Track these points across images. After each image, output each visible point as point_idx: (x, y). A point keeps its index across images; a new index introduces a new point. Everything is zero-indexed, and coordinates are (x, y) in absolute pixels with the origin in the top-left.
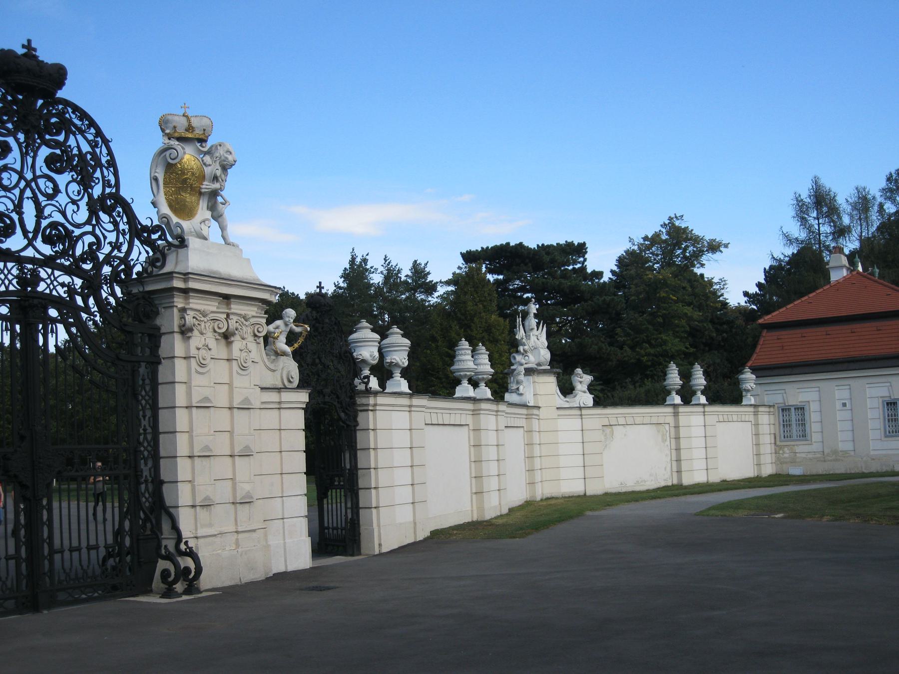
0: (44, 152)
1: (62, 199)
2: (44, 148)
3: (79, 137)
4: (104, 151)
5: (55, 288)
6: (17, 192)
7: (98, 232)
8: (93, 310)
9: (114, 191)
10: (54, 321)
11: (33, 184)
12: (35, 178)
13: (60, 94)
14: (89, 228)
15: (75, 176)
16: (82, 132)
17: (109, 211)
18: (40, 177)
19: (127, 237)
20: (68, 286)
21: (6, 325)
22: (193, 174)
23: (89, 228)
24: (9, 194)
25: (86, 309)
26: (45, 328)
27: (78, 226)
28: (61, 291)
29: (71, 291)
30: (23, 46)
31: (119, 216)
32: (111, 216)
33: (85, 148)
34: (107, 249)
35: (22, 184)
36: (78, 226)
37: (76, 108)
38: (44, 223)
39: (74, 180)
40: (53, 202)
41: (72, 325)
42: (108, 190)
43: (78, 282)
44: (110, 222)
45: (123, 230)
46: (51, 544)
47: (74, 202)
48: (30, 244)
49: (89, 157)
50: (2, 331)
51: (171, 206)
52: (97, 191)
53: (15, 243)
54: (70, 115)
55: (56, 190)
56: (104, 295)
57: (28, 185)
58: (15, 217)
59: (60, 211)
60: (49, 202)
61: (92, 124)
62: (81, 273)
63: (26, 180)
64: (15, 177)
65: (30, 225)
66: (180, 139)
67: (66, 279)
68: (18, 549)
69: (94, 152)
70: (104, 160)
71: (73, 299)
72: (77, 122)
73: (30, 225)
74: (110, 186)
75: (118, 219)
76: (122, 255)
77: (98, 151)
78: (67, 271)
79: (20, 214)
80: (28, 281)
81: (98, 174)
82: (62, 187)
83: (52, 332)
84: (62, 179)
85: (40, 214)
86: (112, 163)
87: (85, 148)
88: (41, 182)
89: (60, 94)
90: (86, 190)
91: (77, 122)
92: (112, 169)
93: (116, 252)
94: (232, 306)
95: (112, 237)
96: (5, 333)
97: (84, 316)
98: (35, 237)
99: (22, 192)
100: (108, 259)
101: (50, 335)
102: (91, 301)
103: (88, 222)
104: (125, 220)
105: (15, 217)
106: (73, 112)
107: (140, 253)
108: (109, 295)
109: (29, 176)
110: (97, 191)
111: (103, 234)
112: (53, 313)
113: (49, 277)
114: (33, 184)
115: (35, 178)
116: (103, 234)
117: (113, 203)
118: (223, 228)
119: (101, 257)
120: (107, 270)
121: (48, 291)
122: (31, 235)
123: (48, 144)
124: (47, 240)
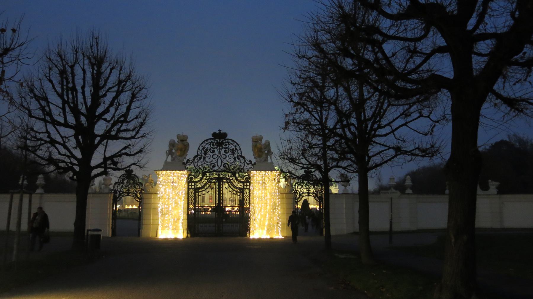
0: (223, 150)
1: (227, 158)
17: (239, 159)
33: (233, 147)
37: (231, 140)
52: (236, 156)
53: (216, 168)
54: (230, 141)
55: (226, 157)
58: (216, 164)
61: (235, 142)
62: (231, 172)
65: (219, 165)
72: (232, 142)
73: (219, 165)
84: (227, 155)
85: (222, 162)
86: (240, 149)
88: (223, 156)
91: (232, 142)
95: (240, 164)
100: (238, 169)
102: (234, 178)
105: (216, 164)
109: (219, 155)
110: (236, 156)
112: (225, 181)
118: (271, 158)
119: (236, 169)
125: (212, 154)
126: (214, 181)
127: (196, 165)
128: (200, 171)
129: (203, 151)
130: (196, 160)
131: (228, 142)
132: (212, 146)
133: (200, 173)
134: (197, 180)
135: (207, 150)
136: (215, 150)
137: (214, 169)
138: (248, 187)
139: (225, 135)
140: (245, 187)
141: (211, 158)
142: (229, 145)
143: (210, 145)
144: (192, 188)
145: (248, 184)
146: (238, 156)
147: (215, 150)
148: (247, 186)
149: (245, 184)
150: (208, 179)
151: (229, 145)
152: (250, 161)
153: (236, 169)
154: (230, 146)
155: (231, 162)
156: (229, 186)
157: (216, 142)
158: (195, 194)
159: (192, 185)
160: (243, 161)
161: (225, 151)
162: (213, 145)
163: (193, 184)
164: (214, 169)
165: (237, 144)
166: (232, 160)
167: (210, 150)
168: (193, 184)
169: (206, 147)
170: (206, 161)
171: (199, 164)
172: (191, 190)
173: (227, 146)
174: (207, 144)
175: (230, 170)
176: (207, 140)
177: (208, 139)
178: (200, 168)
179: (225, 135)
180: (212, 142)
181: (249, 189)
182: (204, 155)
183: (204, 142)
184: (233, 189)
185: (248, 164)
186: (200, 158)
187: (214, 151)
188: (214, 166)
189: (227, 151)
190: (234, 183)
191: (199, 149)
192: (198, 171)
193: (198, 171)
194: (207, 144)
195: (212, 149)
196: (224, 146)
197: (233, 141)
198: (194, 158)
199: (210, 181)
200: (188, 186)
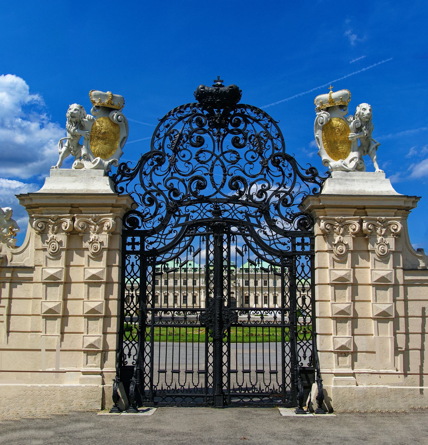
0: (230, 137)
1: (242, 162)
2: (229, 134)
3: (255, 124)
4: (274, 128)
5: (235, 214)
6: (210, 163)
7: (267, 178)
8: (262, 226)
9: (281, 151)
10: (234, 234)
11: (221, 158)
12: (223, 153)
13: (240, 102)
14: (262, 176)
15: (252, 148)
16: (257, 121)
17: (276, 164)
18: (226, 152)
19: (292, 178)
20: (246, 212)
21: (203, 238)
22: (339, 130)
23: (262, 176)
24: (204, 165)
25: (259, 226)
26: (229, 238)
27: (254, 177)
28: (240, 217)
29: (248, 215)
30: (215, 81)
31: (284, 166)
32: (277, 166)
33: (259, 129)
34: (274, 188)
35: (214, 158)
36: (254, 177)
37: (253, 108)
38: (229, 178)
39: (251, 150)
40: (235, 165)
41: (248, 235)
42: (276, 152)
43: (253, 210)
44: (279, 171)
45: (289, 174)
46: (229, 367)
47: (250, 163)
49: (262, 135)
50: (200, 241)
51: (329, 154)
52: (268, 154)
55: (238, 158)
56: (272, 215)
57: (218, 158)
58: (208, 178)
59: (241, 170)
60: (233, 165)
61: (265, 115)
63: (216, 156)
64: (208, 155)
65: (219, 181)
66: (327, 109)
67: (244, 208)
68: (207, 367)
69: (267, 131)
70: (273, 135)
71: (249, 220)
73: (219, 181)
74: (277, 149)
75: (284, 168)
76: (287, 190)
77: (269, 130)
78: (244, 204)
79: (211, 175)
80: (217, 212)
81: (269, 142)
82: (242, 156)
83: (233, 240)
84: (241, 152)
85: (225, 173)
86: (279, 135)
87: (259, 129)
89: (240, 102)
90: (260, 154)
91: (253, 115)
92: (280, 139)
93: (282, 189)
94: (368, 214)
96: (202, 242)
97: (257, 230)
98: (222, 186)
99: (213, 163)
100: (276, 193)
101: (232, 242)
103: (261, 173)
104: (290, 167)
105: (208, 178)
106: (252, 111)
107: (301, 187)
108: (277, 215)
110: (268, 154)
111: (271, 179)
112: (234, 229)
113: (232, 208)
114: (221, 158)
115: (223, 153)
116: (271, 179)
117: (281, 158)
119: (269, 193)
120: (275, 199)
121: (230, 217)
122: (218, 187)
123: (232, 132)
124: (232, 188)
125: (195, 150)
126: (202, 230)
127: (146, 182)
128: (160, 198)
129: (168, 141)
130: (147, 168)
131: (242, 114)
132: (195, 126)
133: (159, 206)
134: (149, 226)
136: (206, 136)
137: (202, 193)
138: (307, 249)
139: (235, 93)
140: (299, 248)
141: (194, 162)
142: (247, 122)
143: (190, 122)
144: (133, 252)
145: (307, 240)
146: (273, 156)
147: (206, 136)
148: (303, 244)
149: (298, 240)
150: (183, 225)
151: (247, 122)
152: (312, 171)
153: (269, 193)
154: (249, 127)
155: (253, 173)
156: (248, 244)
157: (206, 113)
158: (143, 269)
159: (133, 244)
160: (288, 169)
161: (235, 142)
162: (199, 121)
163: (138, 239)
164: (202, 193)
165: (271, 120)
166: (257, 168)
167: (189, 137)
168: (138, 239)
169: (179, 127)
170: (178, 171)
171: (156, 180)
172: (133, 258)
174: (181, 119)
175: (250, 197)
178: (160, 192)
179: (235, 93)
180: (195, 114)
181: (311, 256)
182: (171, 153)
184: (260, 256)
185: (303, 179)
186: (161, 162)
187: (201, 141)
188: (201, 187)
189: (242, 142)
190: (261, 234)
191: (156, 135)
192: (152, 201)
193: (152, 201)
194: (181, 119)
196: (230, 127)
197: (259, 112)
198: (145, 158)
199: (190, 228)
200: (124, 243)
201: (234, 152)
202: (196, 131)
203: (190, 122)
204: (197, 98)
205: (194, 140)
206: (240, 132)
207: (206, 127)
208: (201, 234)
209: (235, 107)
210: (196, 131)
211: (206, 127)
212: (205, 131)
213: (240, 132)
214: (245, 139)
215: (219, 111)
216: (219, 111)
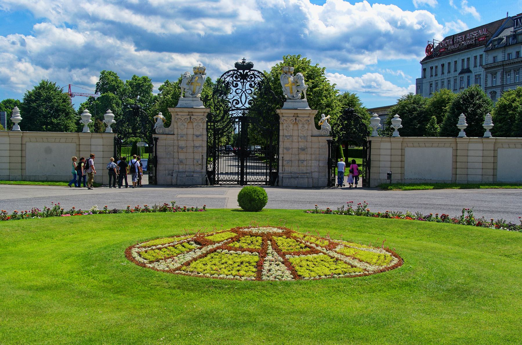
0: (249, 83)
6: (240, 94)
38: (248, 100)
48: (243, 105)
54: (256, 73)
65: (243, 102)
73: (243, 102)
91: (258, 74)
109: (244, 90)
123: (249, 81)
125: (234, 89)
126: (237, 120)
132: (235, 79)
135: (228, 83)
143: (232, 77)
154: (256, 79)
161: (251, 85)
162: (236, 77)
169: (227, 80)
173: (253, 79)
174: (229, 76)
176: (228, 72)
177: (230, 71)
183: (225, 74)
187: (237, 85)
189: (253, 85)
194: (229, 76)
195: (235, 82)
196: (248, 80)
201: (250, 90)
202: (235, 81)
203: (232, 77)
204: (236, 67)
205: (234, 85)
206: (253, 81)
207: (239, 79)
208: (237, 122)
209: (250, 70)
210: (235, 81)
211: (239, 79)
212: (239, 81)
213: (253, 81)
214: (255, 84)
215: (244, 72)
216: (244, 72)
